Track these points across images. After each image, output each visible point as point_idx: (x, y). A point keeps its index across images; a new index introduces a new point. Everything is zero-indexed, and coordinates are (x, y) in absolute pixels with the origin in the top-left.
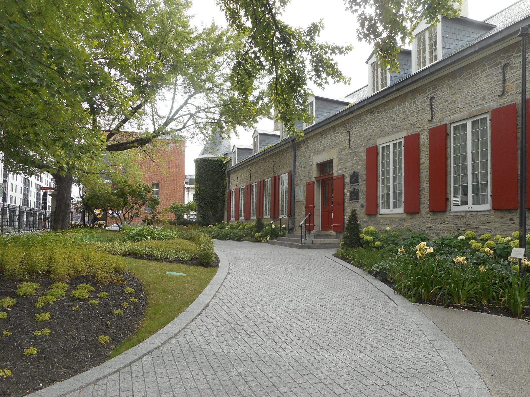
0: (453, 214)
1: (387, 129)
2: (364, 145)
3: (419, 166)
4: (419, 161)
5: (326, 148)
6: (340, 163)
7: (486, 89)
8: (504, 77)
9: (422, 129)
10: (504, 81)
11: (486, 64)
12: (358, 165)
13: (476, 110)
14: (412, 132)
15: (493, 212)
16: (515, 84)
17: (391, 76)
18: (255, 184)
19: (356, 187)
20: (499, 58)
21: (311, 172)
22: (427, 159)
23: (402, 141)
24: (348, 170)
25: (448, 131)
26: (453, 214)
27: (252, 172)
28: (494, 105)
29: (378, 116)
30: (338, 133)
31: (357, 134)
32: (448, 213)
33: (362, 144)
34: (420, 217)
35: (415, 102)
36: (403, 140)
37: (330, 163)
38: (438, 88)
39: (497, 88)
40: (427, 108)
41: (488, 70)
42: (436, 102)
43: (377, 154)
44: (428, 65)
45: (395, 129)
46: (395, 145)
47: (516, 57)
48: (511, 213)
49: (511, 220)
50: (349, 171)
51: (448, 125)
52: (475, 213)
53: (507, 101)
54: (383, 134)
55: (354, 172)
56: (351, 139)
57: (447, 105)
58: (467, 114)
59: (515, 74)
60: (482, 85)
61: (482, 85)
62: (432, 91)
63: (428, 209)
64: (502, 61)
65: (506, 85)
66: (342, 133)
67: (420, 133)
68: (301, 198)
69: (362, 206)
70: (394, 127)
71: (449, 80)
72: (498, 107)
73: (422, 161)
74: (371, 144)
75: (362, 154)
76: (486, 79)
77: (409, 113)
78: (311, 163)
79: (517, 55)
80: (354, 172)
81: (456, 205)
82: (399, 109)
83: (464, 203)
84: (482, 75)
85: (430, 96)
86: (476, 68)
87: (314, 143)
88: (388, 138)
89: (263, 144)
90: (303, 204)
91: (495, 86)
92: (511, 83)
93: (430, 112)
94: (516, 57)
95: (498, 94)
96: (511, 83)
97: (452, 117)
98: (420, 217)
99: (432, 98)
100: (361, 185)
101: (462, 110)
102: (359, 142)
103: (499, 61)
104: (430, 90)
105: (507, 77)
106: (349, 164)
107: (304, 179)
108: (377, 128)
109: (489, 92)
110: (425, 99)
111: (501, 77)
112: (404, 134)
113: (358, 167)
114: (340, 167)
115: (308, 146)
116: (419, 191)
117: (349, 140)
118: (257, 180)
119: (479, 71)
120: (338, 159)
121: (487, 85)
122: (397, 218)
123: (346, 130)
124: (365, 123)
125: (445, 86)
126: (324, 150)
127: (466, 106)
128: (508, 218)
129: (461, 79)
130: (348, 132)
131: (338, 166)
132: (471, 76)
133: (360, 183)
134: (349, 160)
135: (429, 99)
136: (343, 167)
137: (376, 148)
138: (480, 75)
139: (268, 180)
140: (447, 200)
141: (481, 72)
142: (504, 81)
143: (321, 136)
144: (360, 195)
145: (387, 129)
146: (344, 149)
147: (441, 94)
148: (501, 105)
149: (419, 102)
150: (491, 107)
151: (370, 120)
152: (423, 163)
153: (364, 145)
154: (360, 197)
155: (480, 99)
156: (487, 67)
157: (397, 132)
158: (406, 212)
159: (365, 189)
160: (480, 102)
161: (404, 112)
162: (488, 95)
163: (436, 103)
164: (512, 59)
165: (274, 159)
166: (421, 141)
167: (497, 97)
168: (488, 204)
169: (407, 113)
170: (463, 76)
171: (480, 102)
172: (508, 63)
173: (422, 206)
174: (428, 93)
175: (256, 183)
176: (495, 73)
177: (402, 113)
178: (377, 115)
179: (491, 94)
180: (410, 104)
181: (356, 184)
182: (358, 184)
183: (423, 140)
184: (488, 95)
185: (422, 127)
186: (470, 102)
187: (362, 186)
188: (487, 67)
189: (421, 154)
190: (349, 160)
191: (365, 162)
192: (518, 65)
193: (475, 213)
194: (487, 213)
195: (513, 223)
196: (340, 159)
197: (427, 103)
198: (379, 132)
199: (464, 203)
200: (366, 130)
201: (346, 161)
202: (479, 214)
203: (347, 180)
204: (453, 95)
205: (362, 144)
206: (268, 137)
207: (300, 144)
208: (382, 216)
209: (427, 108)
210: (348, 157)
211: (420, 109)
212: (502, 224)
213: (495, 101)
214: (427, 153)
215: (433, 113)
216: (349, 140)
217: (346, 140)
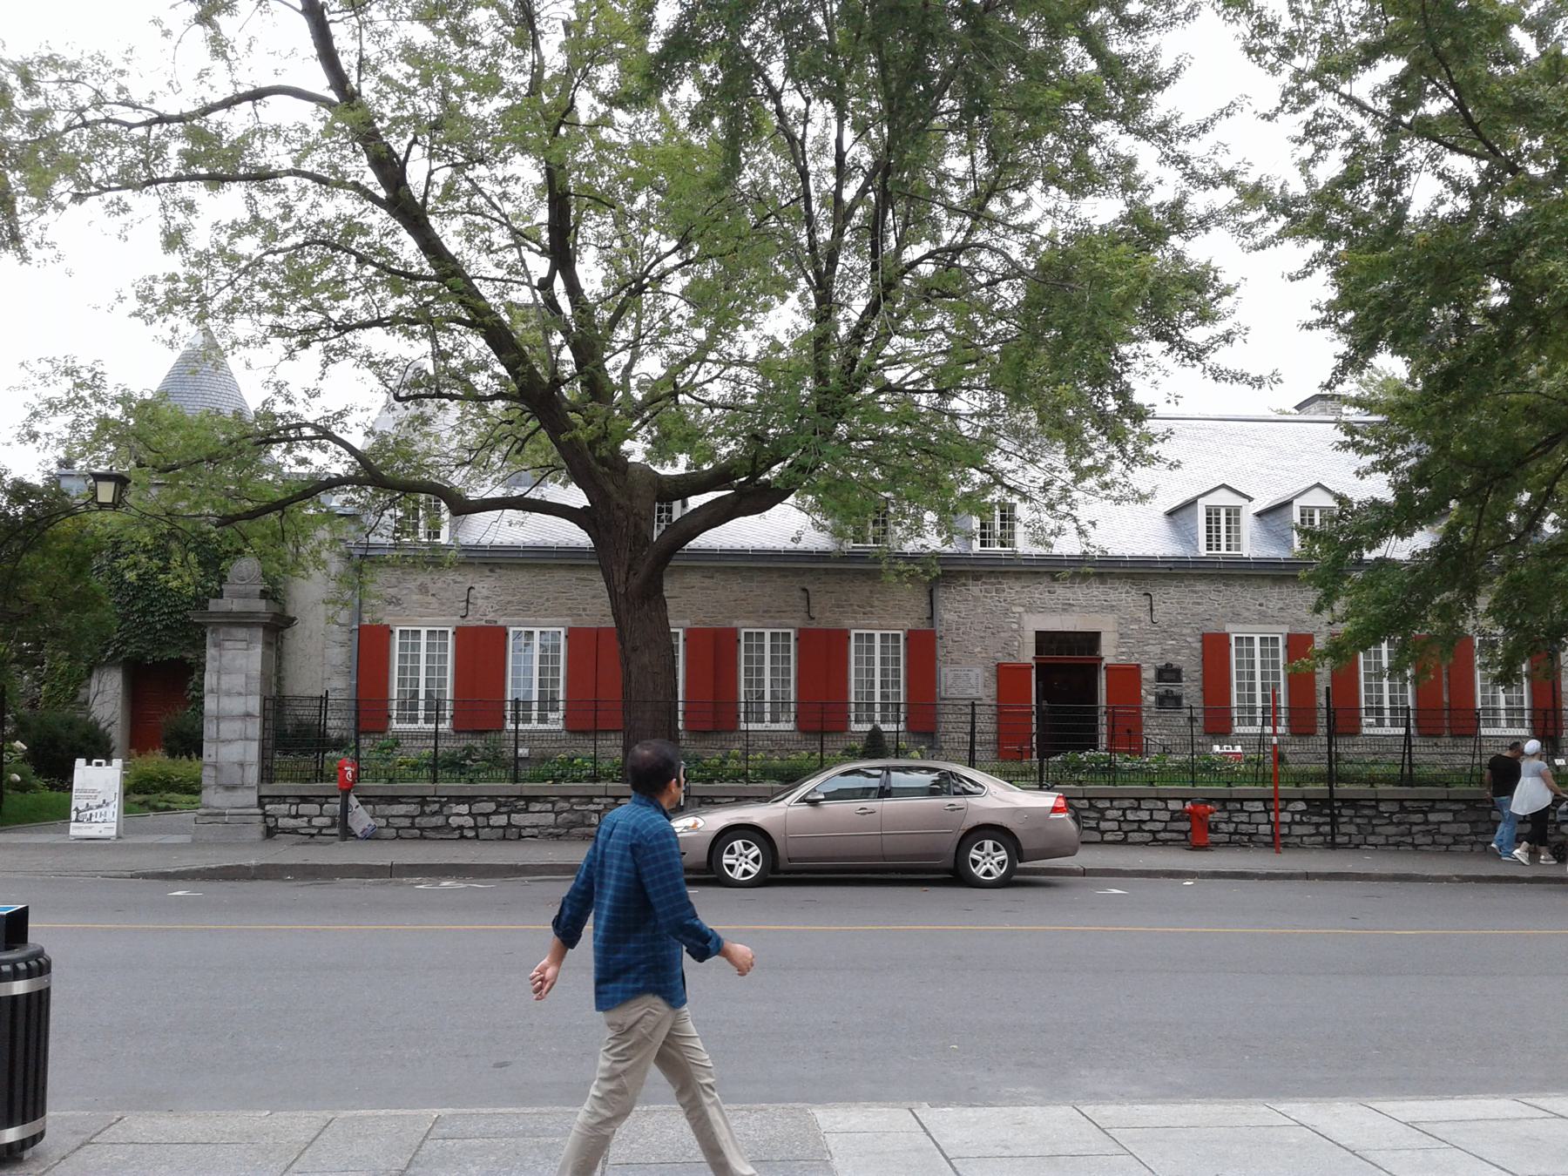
12: (1178, 654)
37: (1092, 639)
45: (1263, 618)
54: (1236, 617)
66: (1127, 592)
74: (1212, 628)
78: (1015, 626)
81: (1370, 725)
83: (1380, 723)
88: (1249, 628)
117: (1151, 609)
120: (1117, 635)
124: (1196, 592)
126: (1064, 610)
131: (1118, 647)
137: (1227, 636)
145: (1247, 614)
187: (1191, 690)
191: (1198, 653)
199: (1380, 723)
200: (1199, 604)
203: (1149, 674)
216: (1151, 609)
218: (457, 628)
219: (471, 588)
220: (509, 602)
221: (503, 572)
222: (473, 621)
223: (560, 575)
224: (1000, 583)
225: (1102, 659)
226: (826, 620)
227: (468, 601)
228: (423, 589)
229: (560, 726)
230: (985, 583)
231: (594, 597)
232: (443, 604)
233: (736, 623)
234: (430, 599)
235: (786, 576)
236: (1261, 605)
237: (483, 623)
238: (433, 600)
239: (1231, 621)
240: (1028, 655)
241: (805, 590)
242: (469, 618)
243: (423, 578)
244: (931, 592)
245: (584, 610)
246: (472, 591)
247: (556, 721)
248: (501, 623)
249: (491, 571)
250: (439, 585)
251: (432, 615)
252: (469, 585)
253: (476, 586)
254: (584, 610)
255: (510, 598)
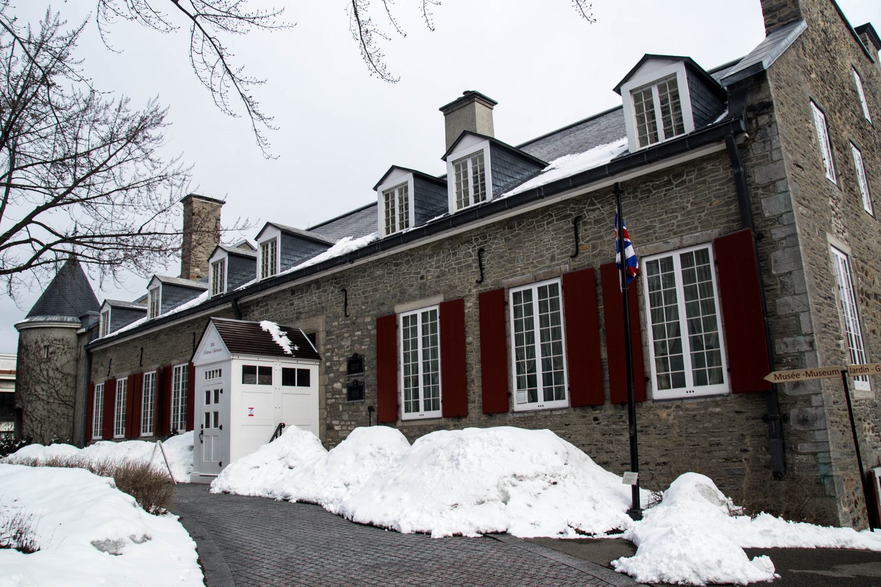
0: (517, 416)
1: (411, 290)
2: (372, 313)
3: (465, 348)
4: (465, 340)
5: (303, 316)
6: (330, 340)
7: (555, 246)
8: (576, 234)
9: (467, 293)
10: (577, 239)
11: (553, 214)
12: (362, 344)
13: (543, 273)
14: (452, 296)
15: (571, 410)
16: (590, 243)
17: (415, 213)
18: (151, 373)
19: (360, 379)
20: (568, 209)
22: (476, 337)
23: (436, 310)
24: (345, 352)
25: (506, 297)
26: (517, 416)
27: (145, 351)
28: (566, 268)
29: (396, 269)
30: (325, 291)
31: (359, 295)
32: (511, 415)
33: (370, 311)
34: (468, 422)
35: (455, 254)
36: (437, 308)
38: (488, 237)
39: (568, 246)
40: (475, 265)
41: (555, 222)
42: (487, 257)
43: (396, 327)
44: (472, 204)
45: (424, 293)
46: (424, 315)
47: (590, 210)
48: (595, 411)
49: (596, 419)
50: (346, 354)
51: (506, 291)
52: (548, 413)
53: (581, 262)
54: (403, 297)
55: (356, 355)
56: (348, 302)
57: (503, 263)
58: (532, 277)
59: (589, 232)
60: (549, 241)
61: (549, 241)
62: (480, 240)
63: (481, 410)
64: (573, 213)
65: (579, 244)
66: (333, 292)
67: (465, 299)
69: (371, 409)
70: (423, 287)
71: (504, 229)
72: (572, 271)
73: (469, 339)
74: (385, 310)
75: (370, 327)
76: (552, 233)
77: (447, 270)
79: (590, 208)
80: (356, 355)
82: (430, 262)
84: (548, 228)
85: (477, 247)
86: (540, 217)
87: (278, 304)
88: (412, 305)
89: (168, 302)
91: (566, 244)
92: (586, 242)
93: (478, 270)
94: (590, 210)
95: (570, 254)
96: (586, 242)
97: (510, 280)
98: (468, 422)
99: (481, 251)
100: (368, 376)
101: (524, 271)
102: (364, 308)
103: (569, 212)
104: (476, 240)
105: (580, 235)
106: (346, 343)
108: (394, 288)
109: (559, 251)
110: (470, 250)
111: (572, 233)
112: (440, 299)
113: (363, 347)
114: (329, 347)
116: (466, 384)
118: (157, 366)
119: (545, 223)
121: (555, 242)
122: (431, 425)
124: (373, 279)
125: (498, 236)
127: (530, 266)
128: (592, 418)
129: (520, 229)
130: (344, 290)
131: (325, 345)
132: (534, 227)
133: (367, 373)
134: (346, 335)
135: (477, 251)
136: (335, 346)
137: (393, 317)
138: (546, 227)
139: (181, 366)
140: (509, 395)
141: (548, 224)
142: (577, 239)
144: (366, 391)
146: (337, 317)
147: (494, 246)
148: (575, 269)
149: (461, 254)
150: (563, 269)
151: (383, 275)
152: (470, 344)
153: (372, 313)
154: (367, 395)
155: (547, 259)
156: (554, 218)
157: (429, 296)
158: (445, 415)
159: (375, 382)
160: (548, 263)
161: (439, 267)
162: (558, 254)
163: (487, 258)
164: (585, 212)
165: (194, 329)
166: (466, 311)
167: (569, 258)
168: (564, 398)
169: (443, 268)
170: (524, 227)
171: (548, 263)
172: (580, 217)
173: (470, 406)
174: (475, 244)
175: (155, 372)
176: (565, 227)
177: (436, 268)
178: (394, 268)
179: (562, 253)
180: (447, 257)
181: (360, 374)
182: (362, 374)
183: (470, 310)
184: (558, 254)
185: (467, 290)
186: (535, 261)
188: (554, 218)
189: (467, 329)
192: (593, 221)
193: (548, 413)
194: (565, 412)
195: (598, 424)
196: (328, 333)
197: (474, 258)
198: (399, 294)
199: (533, 397)
200: (376, 290)
201: (340, 337)
202: (554, 413)
204: (510, 249)
205: (370, 311)
206: (178, 290)
207: (249, 307)
208: (406, 424)
209: (475, 265)
210: (344, 330)
211: (463, 265)
212: (584, 426)
213: (567, 263)
214: (476, 328)
215: (484, 271)
217: (340, 303)
236: (422, 278)
239: (400, 302)
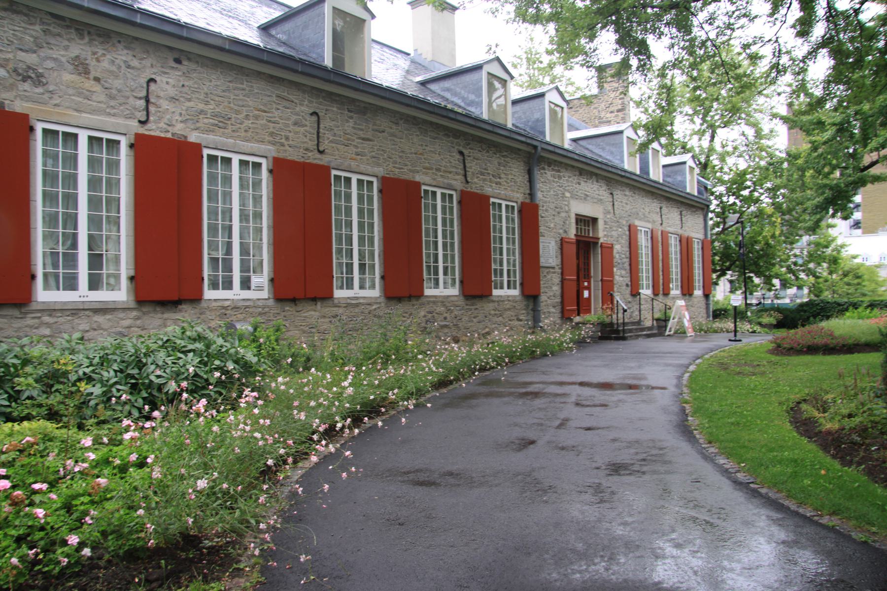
5: (588, 198)
21: (567, 222)
68: (551, 261)
69: (627, 285)
78: (567, 208)
90: (554, 273)
107: (554, 230)
114: (605, 233)
115: (560, 177)
117: (613, 205)
123: (609, 189)
126: (585, 199)
131: (604, 231)
134: (615, 229)
143: (581, 174)
190: (615, 229)
218: (137, 136)
219: (152, 80)
220: (202, 112)
221: (193, 66)
222: (154, 129)
223: (258, 86)
224: (559, 171)
225: (598, 239)
226: (478, 185)
227: (148, 101)
228: (81, 67)
229: (265, 294)
230: (553, 170)
231: (295, 124)
232: (112, 97)
233: (418, 178)
234: (90, 84)
235: (449, 136)
237: (169, 136)
238: (97, 88)
240: (572, 233)
241: (461, 153)
242: (149, 126)
243: (78, 48)
244: (530, 173)
245: (287, 138)
246: (153, 86)
247: (260, 288)
248: (193, 138)
249: (178, 61)
250: (105, 64)
251: (93, 112)
252: (148, 74)
253: (158, 79)
254: (287, 138)
255: (201, 106)
